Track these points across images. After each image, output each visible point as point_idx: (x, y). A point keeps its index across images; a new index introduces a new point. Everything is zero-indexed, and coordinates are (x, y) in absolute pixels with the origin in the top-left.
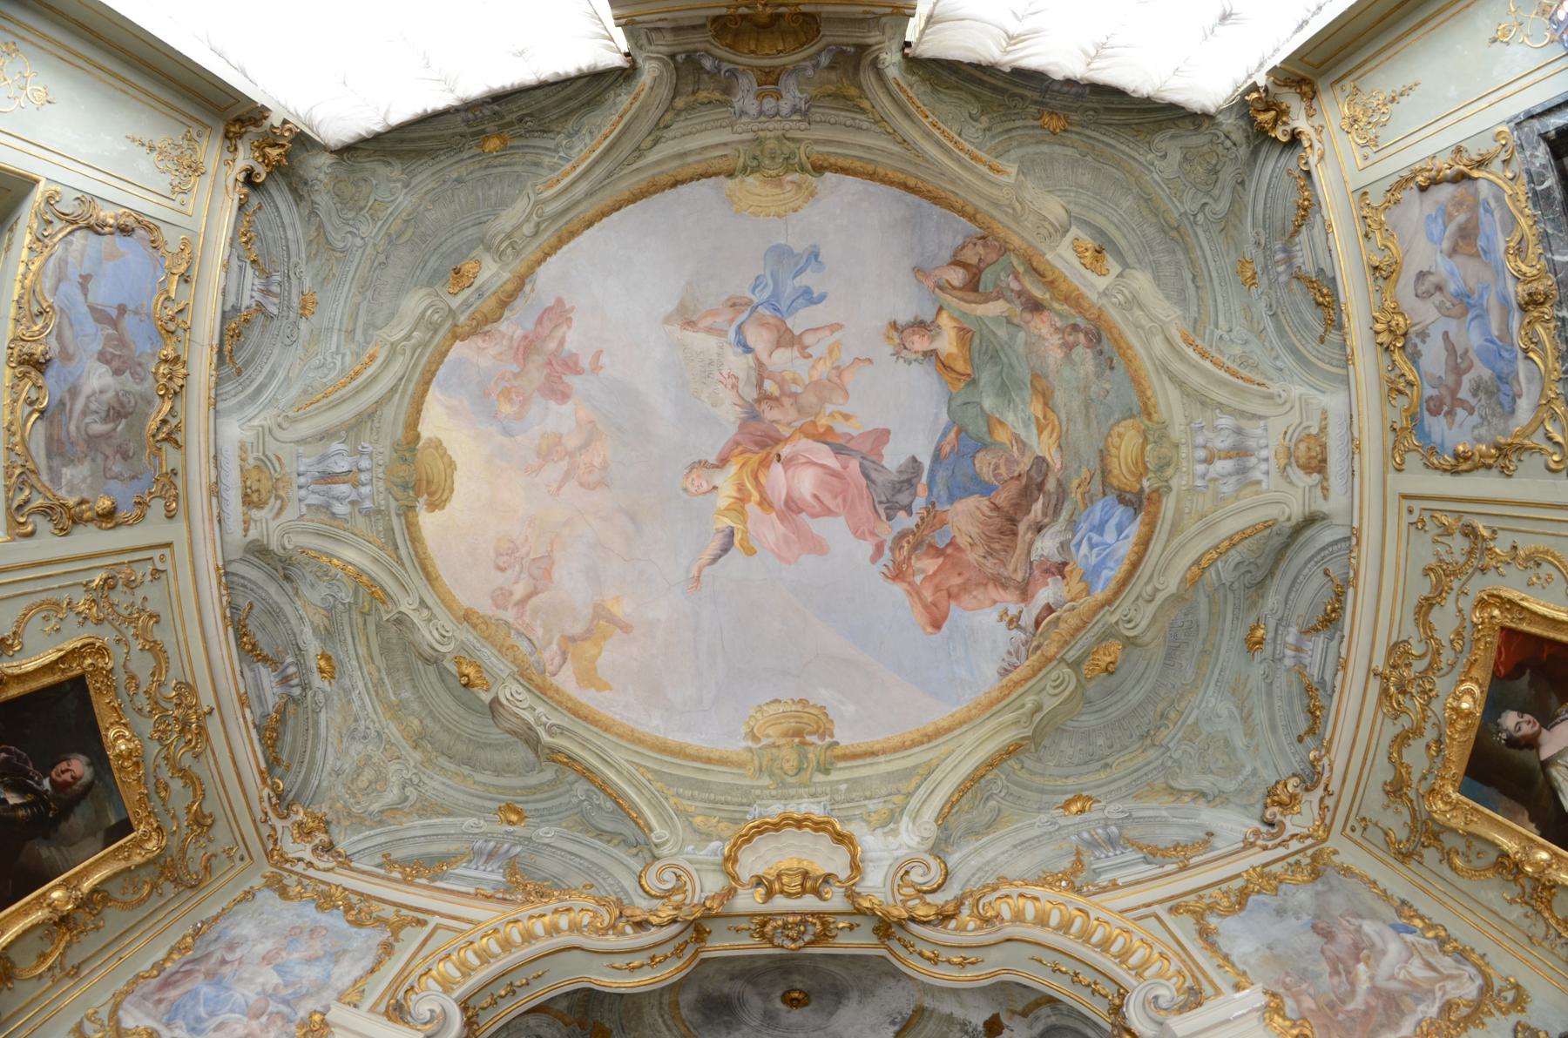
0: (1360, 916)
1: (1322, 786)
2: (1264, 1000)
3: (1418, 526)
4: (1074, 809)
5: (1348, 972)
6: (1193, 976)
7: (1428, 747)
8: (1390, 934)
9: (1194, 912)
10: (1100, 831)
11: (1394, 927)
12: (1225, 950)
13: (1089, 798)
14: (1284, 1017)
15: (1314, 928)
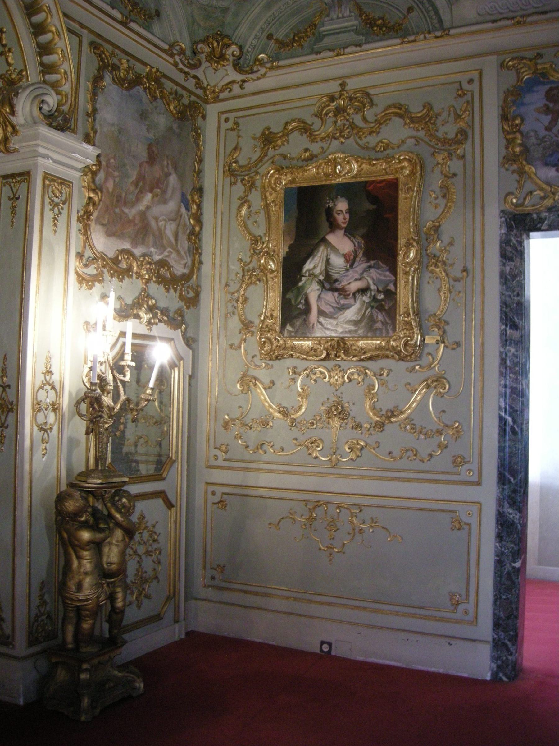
0: (175, 169)
1: (243, 77)
3: (461, 93)
5: (141, 192)
7: (306, 150)
8: (178, 196)
9: (102, 60)
11: (183, 195)
12: (98, 106)
15: (150, 148)
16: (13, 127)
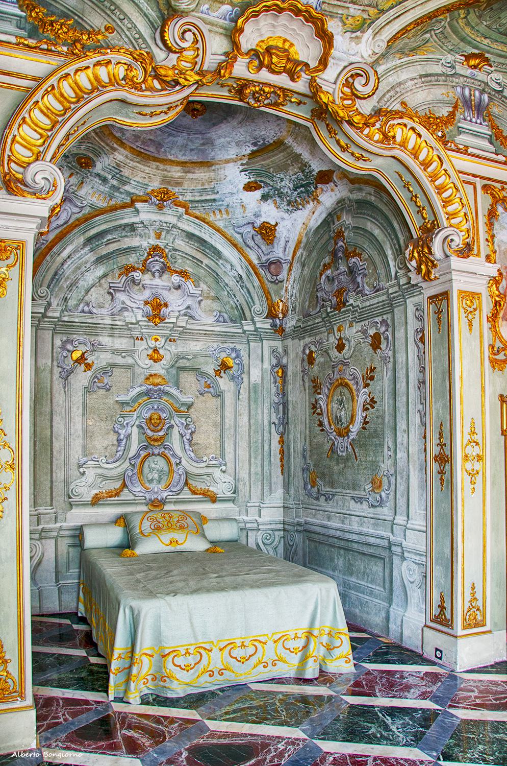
2: (496, 274)
4: (472, 62)
6: (473, 238)
10: (477, 93)
12: (495, 232)
13: (487, 60)
14: (497, 289)
16: (432, 262)
